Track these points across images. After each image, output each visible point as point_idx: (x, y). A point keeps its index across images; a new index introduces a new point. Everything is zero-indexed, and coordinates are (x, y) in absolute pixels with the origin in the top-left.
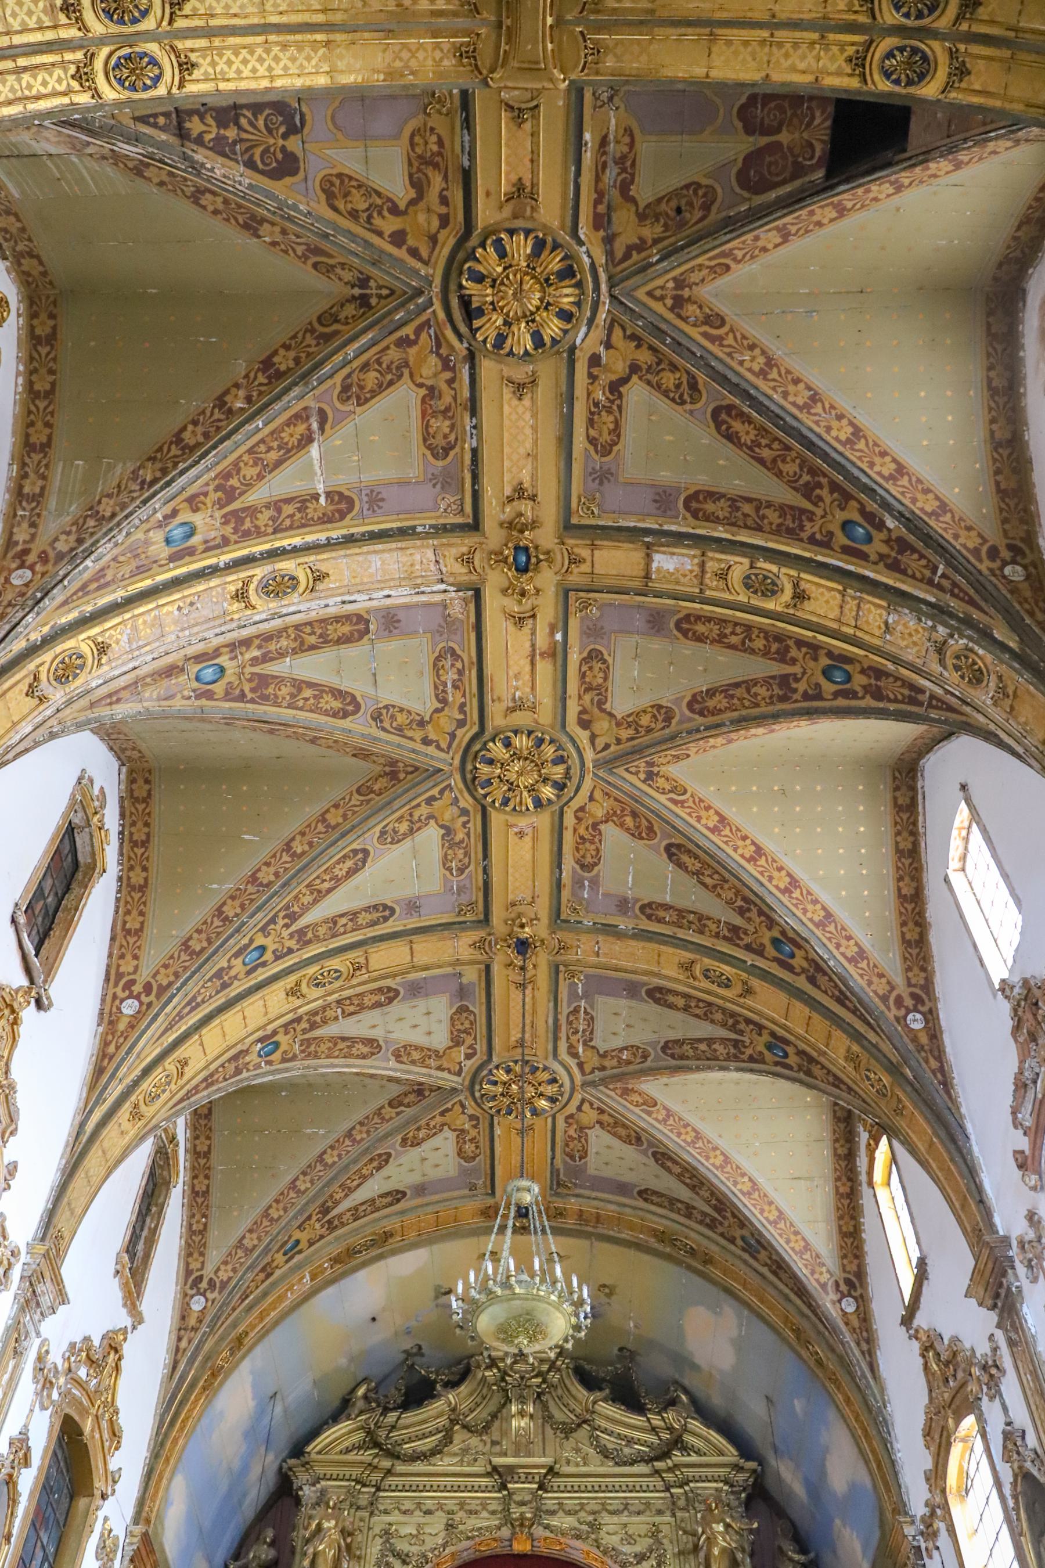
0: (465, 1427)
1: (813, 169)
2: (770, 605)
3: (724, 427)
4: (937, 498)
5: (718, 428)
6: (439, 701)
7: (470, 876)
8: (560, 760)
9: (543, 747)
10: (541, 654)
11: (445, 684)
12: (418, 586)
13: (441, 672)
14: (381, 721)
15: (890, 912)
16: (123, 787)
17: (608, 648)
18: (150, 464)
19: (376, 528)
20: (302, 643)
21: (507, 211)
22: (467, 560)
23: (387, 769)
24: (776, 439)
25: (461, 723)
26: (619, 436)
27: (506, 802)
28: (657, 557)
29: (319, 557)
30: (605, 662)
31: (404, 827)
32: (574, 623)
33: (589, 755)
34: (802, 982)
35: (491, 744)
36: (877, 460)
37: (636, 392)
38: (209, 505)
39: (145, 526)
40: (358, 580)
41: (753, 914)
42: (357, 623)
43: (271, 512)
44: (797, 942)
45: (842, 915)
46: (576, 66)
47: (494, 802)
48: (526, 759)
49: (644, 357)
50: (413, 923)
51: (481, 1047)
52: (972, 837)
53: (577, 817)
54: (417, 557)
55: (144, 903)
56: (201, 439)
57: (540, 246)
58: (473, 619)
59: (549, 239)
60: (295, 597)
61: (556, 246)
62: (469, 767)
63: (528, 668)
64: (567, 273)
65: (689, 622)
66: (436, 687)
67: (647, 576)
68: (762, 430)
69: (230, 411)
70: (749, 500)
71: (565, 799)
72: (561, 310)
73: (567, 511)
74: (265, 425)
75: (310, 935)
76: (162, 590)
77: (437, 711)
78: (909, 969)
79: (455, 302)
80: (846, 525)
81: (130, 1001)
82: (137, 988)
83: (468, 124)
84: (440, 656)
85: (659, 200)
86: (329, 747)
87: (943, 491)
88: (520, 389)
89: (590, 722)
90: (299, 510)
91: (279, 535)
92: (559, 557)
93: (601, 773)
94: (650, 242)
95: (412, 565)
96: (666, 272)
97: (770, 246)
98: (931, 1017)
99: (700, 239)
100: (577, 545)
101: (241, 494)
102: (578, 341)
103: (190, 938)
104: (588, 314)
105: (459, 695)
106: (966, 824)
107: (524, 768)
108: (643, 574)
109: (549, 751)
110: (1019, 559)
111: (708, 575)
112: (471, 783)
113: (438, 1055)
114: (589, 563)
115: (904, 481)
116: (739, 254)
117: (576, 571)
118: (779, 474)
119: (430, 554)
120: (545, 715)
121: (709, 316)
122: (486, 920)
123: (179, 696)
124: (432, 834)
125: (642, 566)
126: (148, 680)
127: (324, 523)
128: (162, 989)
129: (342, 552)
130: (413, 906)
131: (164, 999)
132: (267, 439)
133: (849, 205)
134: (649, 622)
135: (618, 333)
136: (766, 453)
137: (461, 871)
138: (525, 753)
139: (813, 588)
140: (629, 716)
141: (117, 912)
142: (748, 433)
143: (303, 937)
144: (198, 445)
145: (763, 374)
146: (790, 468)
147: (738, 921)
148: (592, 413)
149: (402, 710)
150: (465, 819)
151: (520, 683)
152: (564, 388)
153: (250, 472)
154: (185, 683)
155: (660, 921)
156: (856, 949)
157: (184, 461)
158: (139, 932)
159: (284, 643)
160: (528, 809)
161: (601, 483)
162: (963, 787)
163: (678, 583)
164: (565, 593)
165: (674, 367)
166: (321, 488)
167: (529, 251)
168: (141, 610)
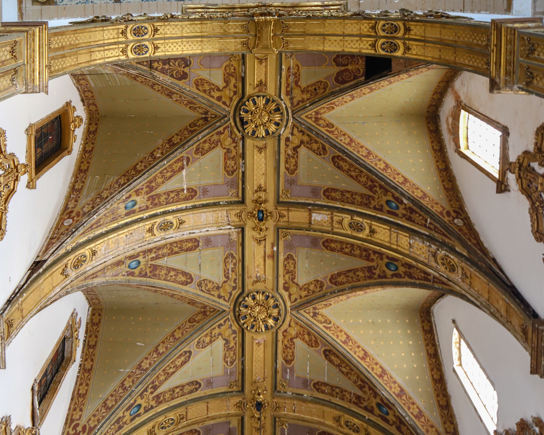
1: (361, 77)
2: (361, 235)
3: (336, 164)
4: (422, 191)
5: (334, 164)
6: (226, 277)
7: (235, 366)
8: (276, 306)
9: (269, 299)
10: (268, 256)
11: (228, 270)
12: (220, 226)
13: (227, 264)
14: (201, 287)
15: (430, 389)
16: (89, 318)
17: (295, 253)
18: (123, 177)
19: (204, 202)
20: (172, 251)
21: (257, 90)
22: (239, 216)
23: (202, 310)
24: (356, 168)
25: (234, 288)
26: (297, 167)
27: (253, 327)
28: (314, 215)
29: (182, 214)
30: (294, 260)
31: (207, 340)
32: (281, 243)
33: (289, 304)
35: (247, 298)
36: (396, 176)
37: (303, 151)
38: (143, 193)
39: (118, 202)
40: (196, 224)
41: (366, 389)
42: (195, 242)
43: (166, 196)
46: (281, 46)
47: (247, 327)
48: (262, 305)
49: (305, 138)
50: (209, 392)
52: (462, 347)
53: (283, 335)
54: (220, 214)
55: (89, 379)
56: (143, 168)
57: (268, 101)
58: (240, 241)
59: (271, 99)
60: (171, 231)
61: (273, 101)
62: (237, 309)
63: (262, 263)
64: (277, 110)
65: (328, 242)
66: (225, 271)
67: (310, 223)
68: (351, 165)
69: (155, 158)
70: (348, 192)
71: (278, 326)
72: (276, 122)
73: (278, 196)
74: (167, 163)
75: (162, 398)
76: (121, 228)
77: (225, 282)
79: (238, 120)
80: (388, 202)
83: (244, 63)
84: (227, 257)
85: (309, 86)
86: (178, 299)
87: (423, 188)
88: (260, 150)
89: (288, 288)
90: (176, 195)
91: (168, 205)
92: (275, 214)
93: (294, 313)
94: (306, 100)
95: (218, 218)
96: (312, 109)
97: (348, 101)
99: (324, 98)
100: (282, 210)
101: (155, 189)
102: (281, 133)
103: (107, 399)
104: (285, 123)
105: (234, 274)
106: (458, 340)
107: (260, 310)
108: (308, 222)
109: (271, 302)
110: (459, 216)
111: (335, 222)
112: (237, 318)
114: (287, 217)
115: (408, 185)
116: (337, 103)
117: (282, 220)
118: (359, 182)
119: (225, 213)
120: (269, 284)
121: (328, 124)
122: (242, 390)
123: (121, 274)
124: (220, 342)
125: (308, 218)
126: (109, 267)
127: (185, 200)
129: (191, 212)
130: (209, 383)
132: (167, 168)
133: (374, 88)
134: (312, 242)
135: (295, 130)
136: (353, 174)
137: (232, 363)
138: (261, 302)
139: (378, 228)
140: (305, 285)
141: (76, 384)
142: (345, 166)
144: (142, 170)
145: (349, 144)
146: (363, 179)
148: (287, 159)
149: (210, 281)
150: (234, 335)
151: (259, 269)
152: (277, 149)
153: (159, 180)
154: (124, 268)
155: (323, 392)
156: (417, 410)
157: (136, 176)
159: (165, 251)
160: (262, 331)
161: (291, 185)
162: (454, 321)
163: (322, 226)
164: (277, 229)
165: (316, 142)
166: (185, 187)
167: (264, 102)
168: (112, 236)
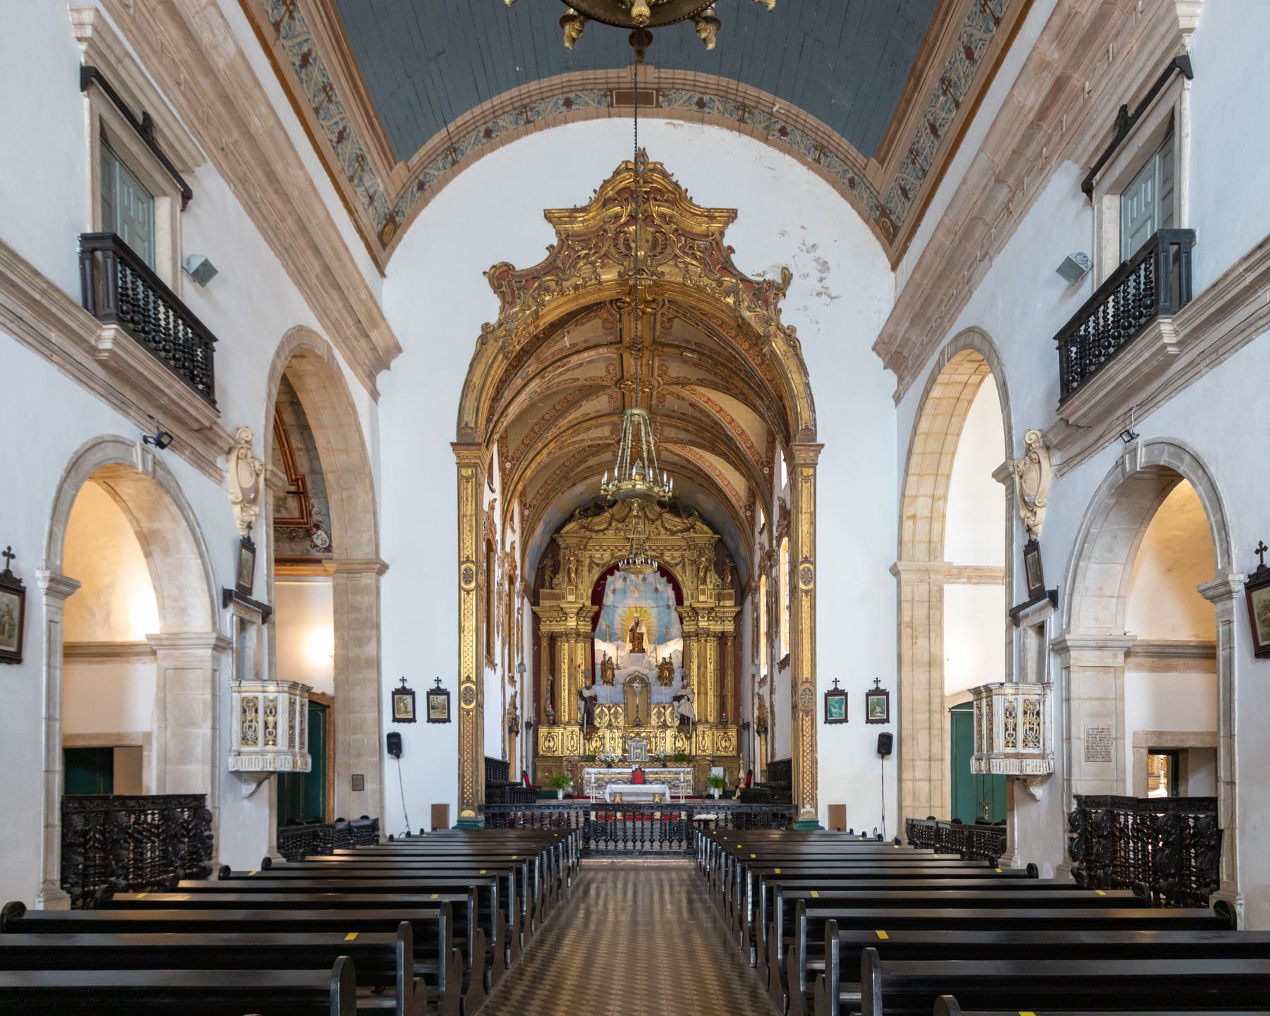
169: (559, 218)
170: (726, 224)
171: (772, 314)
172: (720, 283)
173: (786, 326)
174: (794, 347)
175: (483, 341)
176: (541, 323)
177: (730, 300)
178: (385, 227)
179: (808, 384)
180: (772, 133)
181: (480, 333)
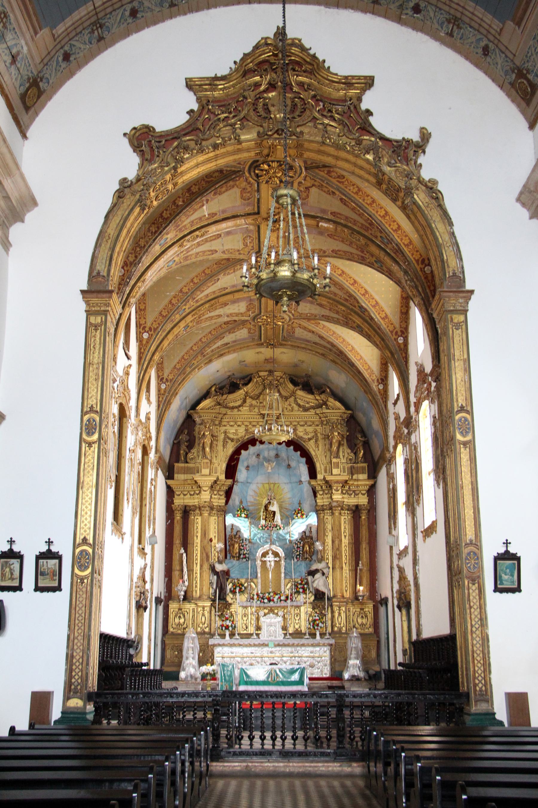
0: (251, 397)
34: (367, 318)
44: (366, 309)
45: (382, 303)
51: (257, 312)
63: (276, 239)
78: (401, 322)
81: (145, 334)
82: (147, 329)
98: (406, 339)
113: (242, 314)
128: (155, 330)
130: (234, 286)
131: (156, 332)
143: (197, 301)
147: (348, 298)
158: (144, 310)
169: (200, 85)
170: (364, 91)
171: (412, 168)
172: (359, 142)
173: (427, 179)
174: (437, 198)
175: (120, 195)
176: (180, 181)
177: (370, 157)
178: (28, 90)
179: (453, 233)
180: (405, 12)
181: (117, 187)
